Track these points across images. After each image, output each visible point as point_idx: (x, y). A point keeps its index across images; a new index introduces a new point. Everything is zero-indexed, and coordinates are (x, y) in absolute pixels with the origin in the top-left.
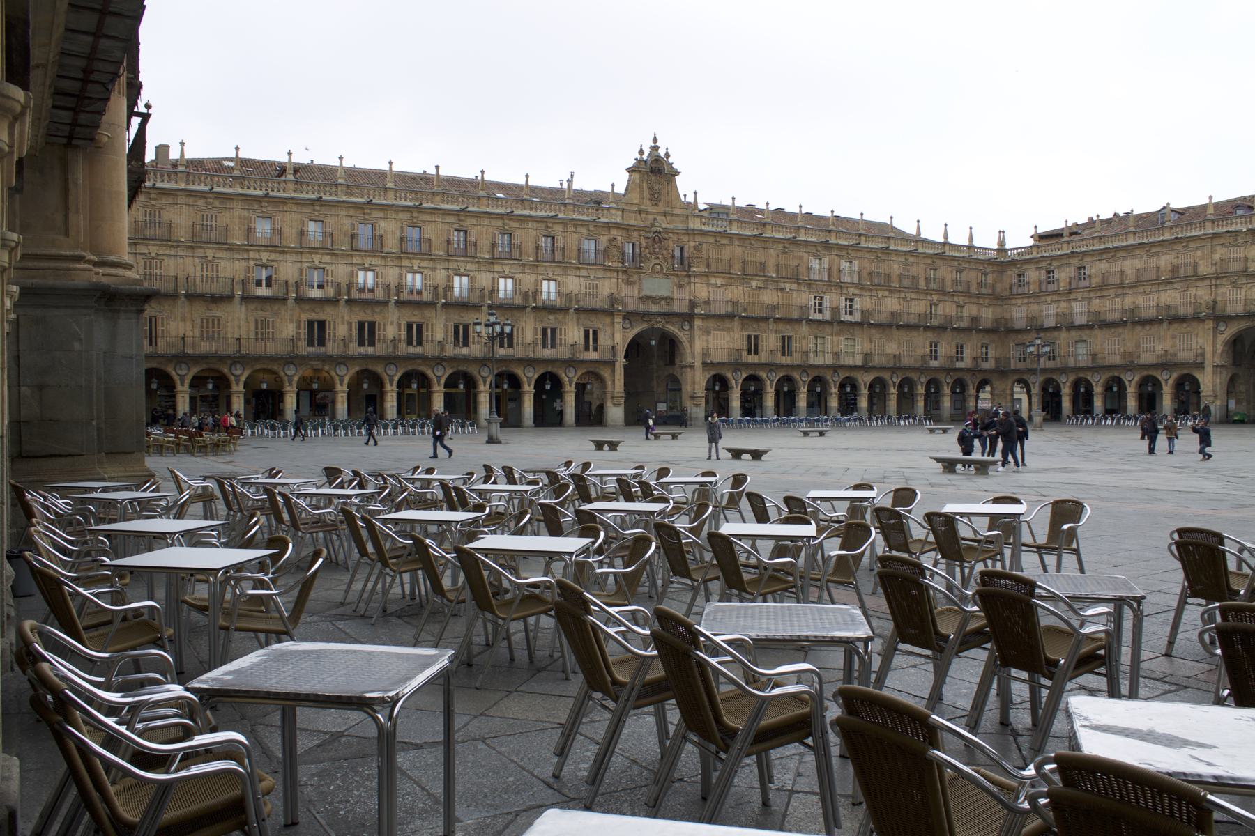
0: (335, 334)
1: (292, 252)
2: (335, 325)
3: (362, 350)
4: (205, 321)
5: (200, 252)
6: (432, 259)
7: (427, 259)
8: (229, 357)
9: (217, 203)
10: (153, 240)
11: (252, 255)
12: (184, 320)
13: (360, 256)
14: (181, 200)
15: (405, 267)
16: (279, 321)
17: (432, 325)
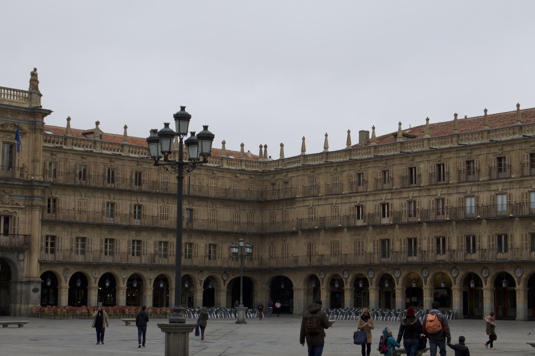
0: (479, 245)
1: (371, 194)
2: (393, 242)
3: (410, 259)
4: (333, 244)
5: (330, 201)
6: (448, 188)
7: (445, 187)
8: (342, 266)
9: (339, 169)
10: (310, 197)
11: (353, 199)
12: (323, 244)
13: (406, 191)
14: (323, 170)
15: (433, 195)
16: (365, 241)
17: (449, 238)
